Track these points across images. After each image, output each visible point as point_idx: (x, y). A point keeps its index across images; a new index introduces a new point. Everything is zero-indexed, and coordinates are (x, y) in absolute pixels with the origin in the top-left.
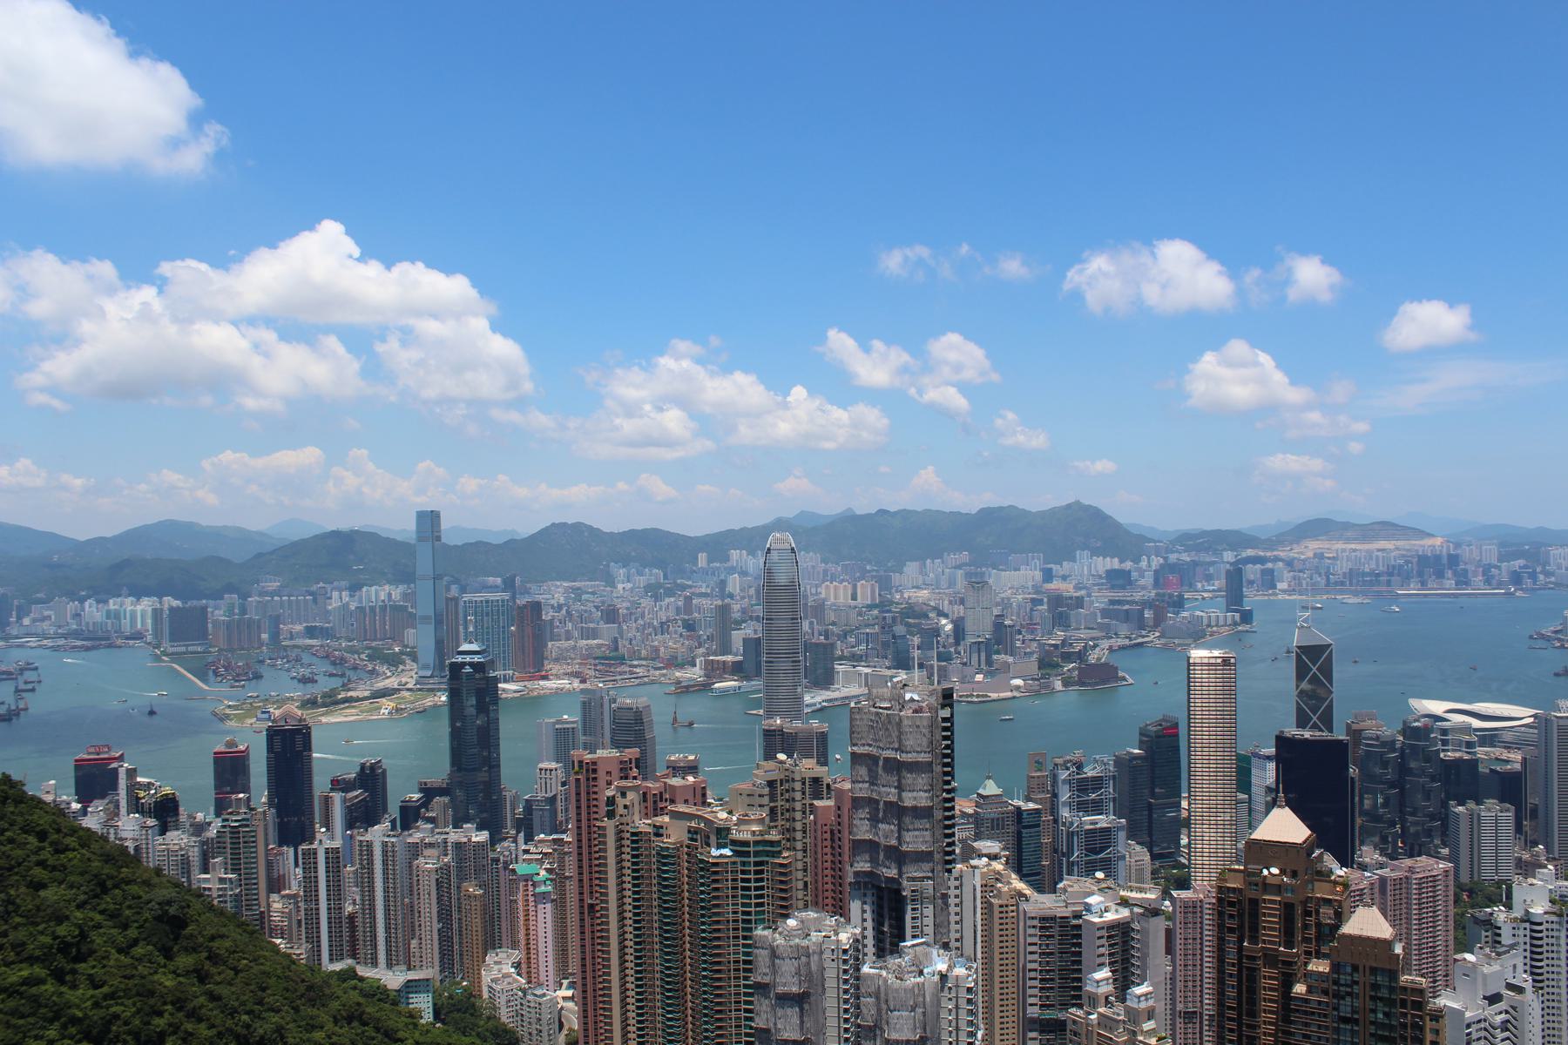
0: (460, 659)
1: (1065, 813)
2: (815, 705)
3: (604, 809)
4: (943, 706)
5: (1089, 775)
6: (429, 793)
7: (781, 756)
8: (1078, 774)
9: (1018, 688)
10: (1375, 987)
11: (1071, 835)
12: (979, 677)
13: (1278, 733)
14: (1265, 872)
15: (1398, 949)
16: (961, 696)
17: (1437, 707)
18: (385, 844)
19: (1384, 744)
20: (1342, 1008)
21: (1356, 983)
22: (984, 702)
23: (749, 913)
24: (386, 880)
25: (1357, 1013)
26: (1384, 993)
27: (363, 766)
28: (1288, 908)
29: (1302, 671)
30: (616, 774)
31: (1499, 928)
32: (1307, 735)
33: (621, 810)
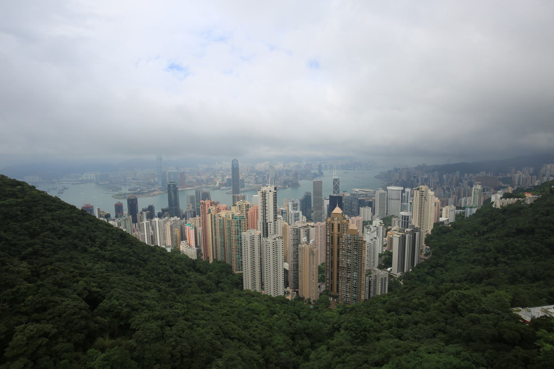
0: (170, 184)
1: (290, 210)
3: (207, 212)
4: (275, 190)
6: (164, 211)
7: (241, 200)
10: (354, 238)
15: (358, 231)
17: (357, 190)
18: (159, 221)
19: (348, 197)
21: (351, 237)
23: (238, 230)
24: (159, 228)
27: (149, 206)
28: (339, 225)
29: (334, 183)
30: (209, 205)
32: (335, 195)
33: (211, 212)
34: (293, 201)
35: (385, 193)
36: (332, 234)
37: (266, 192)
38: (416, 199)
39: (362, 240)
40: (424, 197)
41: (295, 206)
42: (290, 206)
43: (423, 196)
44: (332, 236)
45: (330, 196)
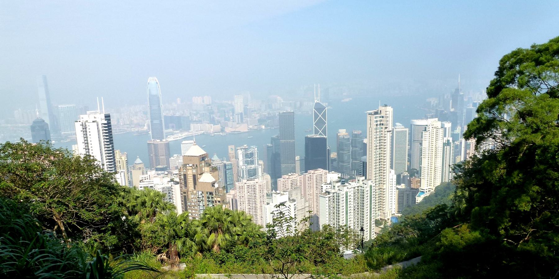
1: (241, 163)
2: (182, 136)
5: (249, 152)
8: (245, 152)
9: (250, 129)
11: (243, 171)
12: (238, 126)
13: (306, 136)
14: (188, 165)
16: (231, 132)
20: (200, 205)
21: (203, 197)
22: (239, 133)
25: (204, 206)
26: (210, 199)
28: (194, 176)
29: (316, 116)
31: (322, 187)
34: (245, 149)
35: (406, 131)
36: (185, 193)
37: (87, 123)
38: (370, 131)
39: (219, 202)
40: (384, 127)
41: (249, 156)
42: (241, 157)
43: (383, 124)
44: (185, 196)
45: (307, 139)
